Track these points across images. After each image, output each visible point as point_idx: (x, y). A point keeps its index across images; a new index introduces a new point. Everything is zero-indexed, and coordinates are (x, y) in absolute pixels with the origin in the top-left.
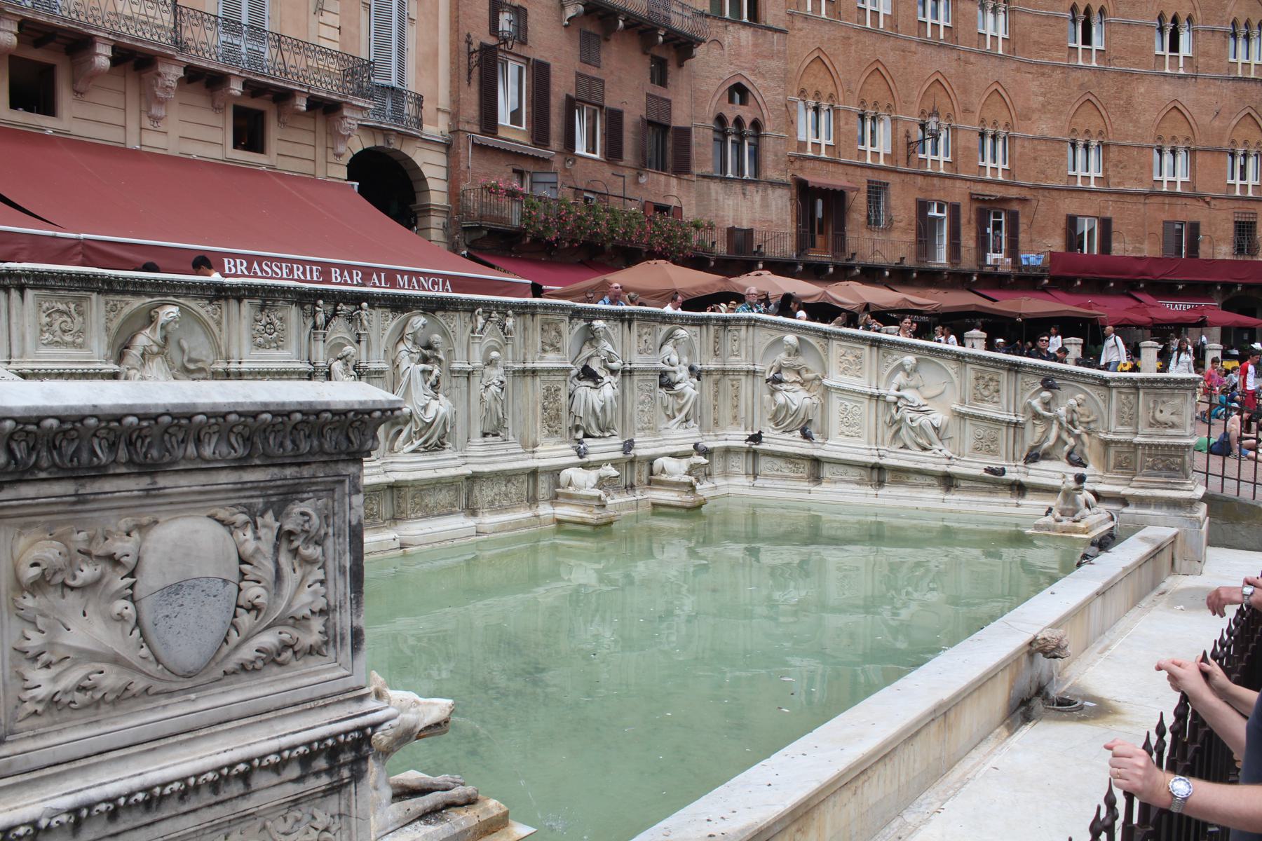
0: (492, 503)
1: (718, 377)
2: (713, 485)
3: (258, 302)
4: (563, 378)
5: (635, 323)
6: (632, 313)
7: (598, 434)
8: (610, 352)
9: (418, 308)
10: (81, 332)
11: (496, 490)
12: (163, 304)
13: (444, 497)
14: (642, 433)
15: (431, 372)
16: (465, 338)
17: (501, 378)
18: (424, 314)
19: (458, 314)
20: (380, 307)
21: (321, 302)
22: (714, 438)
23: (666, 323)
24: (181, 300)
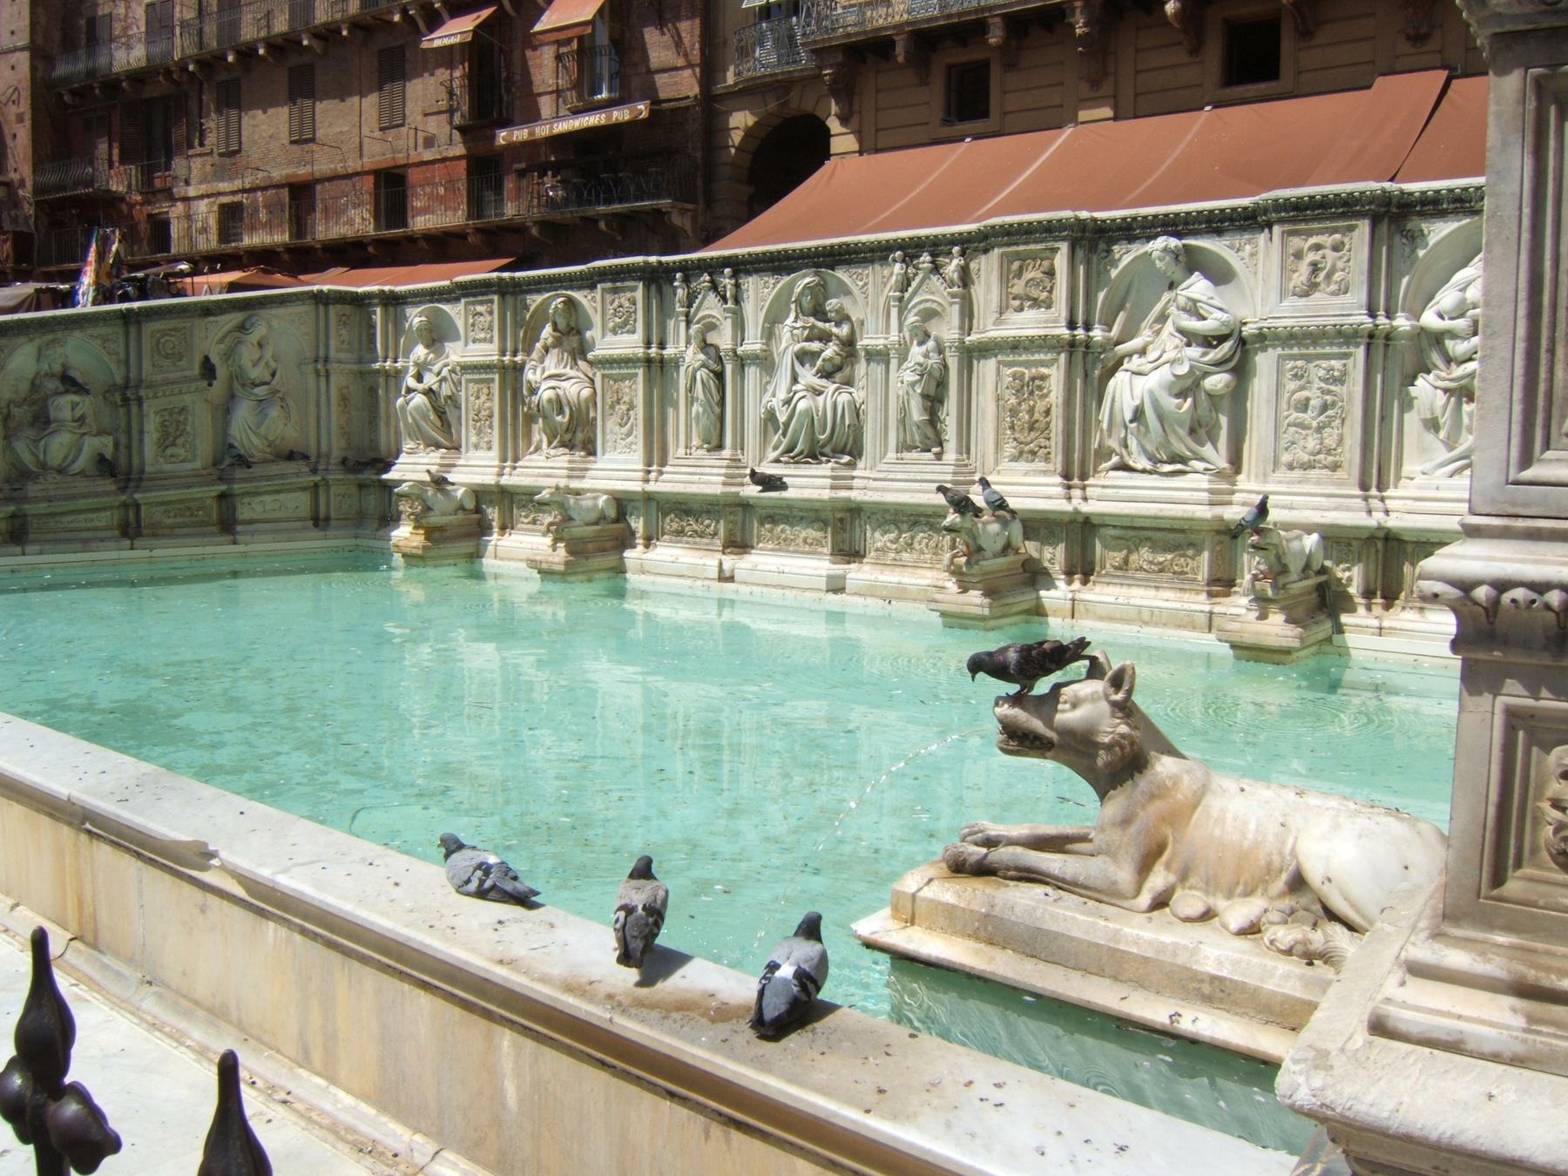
0: (883, 550)
3: (609, 285)
4: (1049, 356)
7: (1142, 463)
8: (1195, 301)
9: (807, 266)
10: (491, 328)
12: (558, 296)
14: (1297, 473)
15: (818, 354)
16: (882, 300)
17: (921, 360)
18: (816, 274)
20: (757, 271)
23: (1442, 214)
24: (569, 293)
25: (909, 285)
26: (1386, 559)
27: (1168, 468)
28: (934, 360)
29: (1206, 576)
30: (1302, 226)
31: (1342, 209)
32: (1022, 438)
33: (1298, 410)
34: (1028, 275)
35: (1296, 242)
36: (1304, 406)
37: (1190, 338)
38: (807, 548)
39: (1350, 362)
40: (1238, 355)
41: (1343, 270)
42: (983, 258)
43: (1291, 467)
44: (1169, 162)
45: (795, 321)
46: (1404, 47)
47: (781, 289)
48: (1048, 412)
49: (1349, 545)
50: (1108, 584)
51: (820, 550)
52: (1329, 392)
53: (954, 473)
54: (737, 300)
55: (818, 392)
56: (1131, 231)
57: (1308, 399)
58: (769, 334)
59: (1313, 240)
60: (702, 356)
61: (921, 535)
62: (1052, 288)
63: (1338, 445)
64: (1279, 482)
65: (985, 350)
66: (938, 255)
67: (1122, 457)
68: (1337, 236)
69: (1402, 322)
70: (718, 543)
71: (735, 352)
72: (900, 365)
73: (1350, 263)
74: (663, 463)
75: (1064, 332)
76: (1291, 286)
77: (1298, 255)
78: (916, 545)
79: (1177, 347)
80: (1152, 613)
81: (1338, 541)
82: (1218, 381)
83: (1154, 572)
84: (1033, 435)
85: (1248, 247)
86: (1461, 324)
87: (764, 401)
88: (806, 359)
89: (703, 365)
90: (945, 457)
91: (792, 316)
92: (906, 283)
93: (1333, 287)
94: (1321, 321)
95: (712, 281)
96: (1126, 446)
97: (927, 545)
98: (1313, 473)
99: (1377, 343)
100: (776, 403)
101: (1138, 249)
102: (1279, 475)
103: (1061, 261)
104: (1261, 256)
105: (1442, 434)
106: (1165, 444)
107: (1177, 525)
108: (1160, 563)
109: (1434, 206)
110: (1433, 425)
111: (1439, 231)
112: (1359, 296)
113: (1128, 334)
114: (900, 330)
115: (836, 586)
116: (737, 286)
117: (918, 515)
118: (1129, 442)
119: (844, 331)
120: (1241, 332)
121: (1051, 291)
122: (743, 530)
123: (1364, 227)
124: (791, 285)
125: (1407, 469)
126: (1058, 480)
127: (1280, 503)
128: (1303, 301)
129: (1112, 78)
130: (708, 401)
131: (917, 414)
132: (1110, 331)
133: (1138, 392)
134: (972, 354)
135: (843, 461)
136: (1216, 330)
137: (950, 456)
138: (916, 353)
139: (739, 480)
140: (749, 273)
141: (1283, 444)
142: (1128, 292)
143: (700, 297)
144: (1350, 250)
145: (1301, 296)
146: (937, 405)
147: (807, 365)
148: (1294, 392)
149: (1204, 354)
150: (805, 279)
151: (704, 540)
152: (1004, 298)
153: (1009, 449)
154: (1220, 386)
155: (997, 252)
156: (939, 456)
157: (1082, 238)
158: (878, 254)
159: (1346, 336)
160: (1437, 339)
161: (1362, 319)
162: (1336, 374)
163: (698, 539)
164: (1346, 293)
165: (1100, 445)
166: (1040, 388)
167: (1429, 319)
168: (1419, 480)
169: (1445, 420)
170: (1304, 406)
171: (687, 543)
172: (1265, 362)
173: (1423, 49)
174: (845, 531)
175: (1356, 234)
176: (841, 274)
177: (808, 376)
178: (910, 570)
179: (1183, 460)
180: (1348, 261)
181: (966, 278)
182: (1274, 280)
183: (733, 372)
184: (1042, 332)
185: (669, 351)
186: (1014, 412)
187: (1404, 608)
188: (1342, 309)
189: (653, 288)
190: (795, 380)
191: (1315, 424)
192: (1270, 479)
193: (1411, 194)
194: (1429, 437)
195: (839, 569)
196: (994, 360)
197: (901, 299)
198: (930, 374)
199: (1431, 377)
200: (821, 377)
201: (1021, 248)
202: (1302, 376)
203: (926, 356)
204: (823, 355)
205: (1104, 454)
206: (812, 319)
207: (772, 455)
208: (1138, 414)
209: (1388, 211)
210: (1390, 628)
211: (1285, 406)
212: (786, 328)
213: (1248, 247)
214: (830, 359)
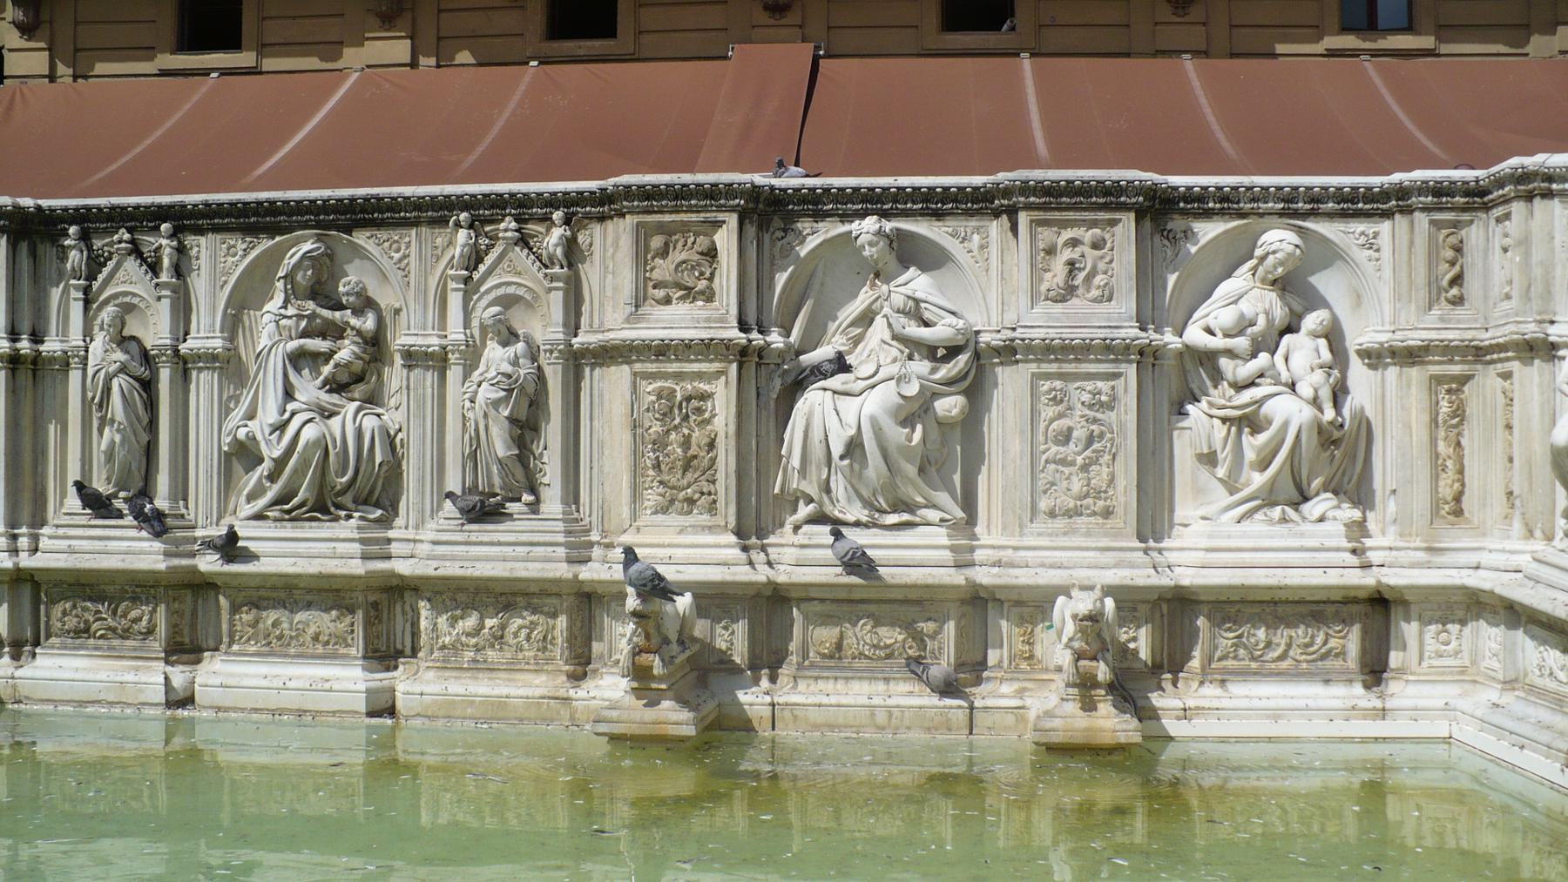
0: (456, 647)
1: (1456, 369)
2: (1378, 704)
4: (716, 366)
5: (1023, 218)
6: (1007, 192)
8: (917, 301)
11: (470, 622)
13: (320, 621)
14: (1060, 523)
16: (433, 282)
17: (508, 368)
18: (319, 238)
19: (414, 232)
20: (216, 229)
21: (72, 230)
22: (1421, 555)
23: (1208, 214)
25: (480, 260)
26: (1170, 624)
27: (892, 519)
28: (526, 368)
29: (952, 660)
30: (1057, 215)
31: (1110, 198)
32: (673, 480)
33: (1057, 442)
34: (677, 256)
35: (1046, 235)
36: (1065, 437)
37: (915, 347)
38: (320, 649)
39: (1119, 383)
40: (973, 372)
41: (1105, 273)
42: (596, 229)
43: (1052, 514)
44: (500, 123)
45: (285, 307)
46: (763, 17)
47: (257, 258)
48: (711, 445)
49: (1135, 609)
50: (817, 678)
51: (343, 651)
52: (1095, 421)
53: (565, 532)
54: (179, 271)
55: (327, 414)
56: (816, 205)
57: (1070, 430)
58: (233, 323)
59: (1068, 234)
60: (119, 356)
61: (519, 622)
62: (712, 274)
63: (1109, 486)
64: (1039, 534)
65: (608, 354)
66: (526, 221)
67: (821, 504)
68: (1097, 231)
69: (1170, 339)
70: (157, 646)
71: (176, 352)
72: (466, 376)
73: (1114, 265)
74: (39, 521)
75: (734, 333)
76: (1043, 288)
77: (1051, 251)
78: (509, 639)
79: (895, 360)
80: (890, 715)
81: (1132, 602)
82: (950, 405)
83: (880, 658)
84: (690, 476)
85: (976, 237)
86: (1242, 343)
87: (229, 425)
88: (302, 362)
89: (123, 369)
90: (543, 507)
91: (279, 299)
92: (475, 258)
93: (1095, 293)
94: (1086, 333)
95: (133, 241)
96: (828, 491)
97: (528, 638)
98: (1081, 521)
99: (1148, 357)
100: (258, 427)
101: (832, 229)
102: (1037, 526)
103: (726, 239)
104: (994, 249)
105: (1221, 472)
106: (889, 487)
107: (913, 595)
108: (887, 647)
109: (1200, 204)
110: (1209, 459)
111: (1208, 231)
112: (1125, 305)
113: (813, 339)
114: (467, 324)
115: (383, 707)
116: (181, 250)
117: (514, 594)
118: (833, 485)
119: (369, 323)
120: (976, 343)
121: (711, 279)
122: (193, 626)
123: (1128, 220)
124: (275, 256)
125: (1180, 514)
126: (733, 539)
127: (1047, 561)
128: (1058, 308)
129: (409, 15)
130: (131, 424)
131: (500, 444)
132: (788, 335)
133: (850, 419)
134: (578, 362)
135: (371, 516)
136: (950, 340)
137: (552, 504)
138: (496, 356)
139: (189, 548)
140: (200, 231)
141: (1041, 484)
142: (808, 286)
143: (111, 265)
144: (1112, 250)
145: (1056, 301)
146: (528, 435)
147: (306, 372)
148: (1052, 421)
149: (934, 371)
150: (305, 244)
151: (129, 643)
152: (641, 286)
153: (652, 497)
154: (955, 412)
155: (630, 220)
156: (534, 507)
157: (754, 210)
158: (437, 213)
159: (1110, 351)
160: (1207, 359)
161: (1131, 332)
162: (1104, 398)
163: (116, 642)
164: (1110, 300)
165: (782, 490)
166: (699, 411)
167: (1195, 335)
168: (1198, 527)
169: (1224, 456)
170: (1065, 437)
171: (97, 648)
172: (1010, 384)
173: (783, 22)
174: (380, 622)
175: (1118, 229)
176: (361, 238)
177: (309, 389)
178: (502, 675)
179: (910, 508)
180: (1111, 261)
181: (571, 251)
182: (1024, 282)
183: (171, 381)
184: (705, 335)
185: (51, 346)
186: (660, 444)
187: (1202, 683)
188: (1109, 320)
189: (24, 247)
190: (289, 395)
191: (1079, 460)
192: (1026, 531)
193: (1176, 188)
194: (1203, 473)
195: (381, 678)
196: (626, 368)
197: (467, 280)
198: (522, 388)
199: (1204, 404)
200: (330, 391)
201: (667, 218)
202: (1062, 401)
203: (515, 363)
204: (336, 356)
205: (792, 501)
206: (311, 306)
207: (248, 509)
208: (854, 447)
209: (1153, 206)
210: (1197, 708)
211: (1041, 438)
212: (267, 317)
213: (976, 237)
214: (348, 365)
